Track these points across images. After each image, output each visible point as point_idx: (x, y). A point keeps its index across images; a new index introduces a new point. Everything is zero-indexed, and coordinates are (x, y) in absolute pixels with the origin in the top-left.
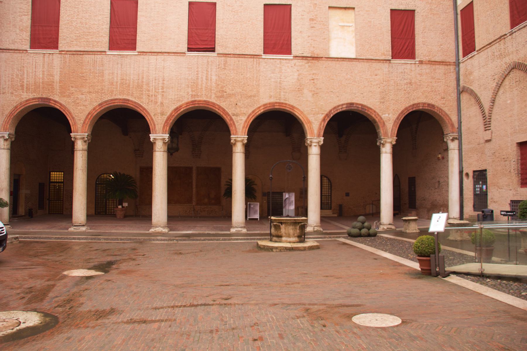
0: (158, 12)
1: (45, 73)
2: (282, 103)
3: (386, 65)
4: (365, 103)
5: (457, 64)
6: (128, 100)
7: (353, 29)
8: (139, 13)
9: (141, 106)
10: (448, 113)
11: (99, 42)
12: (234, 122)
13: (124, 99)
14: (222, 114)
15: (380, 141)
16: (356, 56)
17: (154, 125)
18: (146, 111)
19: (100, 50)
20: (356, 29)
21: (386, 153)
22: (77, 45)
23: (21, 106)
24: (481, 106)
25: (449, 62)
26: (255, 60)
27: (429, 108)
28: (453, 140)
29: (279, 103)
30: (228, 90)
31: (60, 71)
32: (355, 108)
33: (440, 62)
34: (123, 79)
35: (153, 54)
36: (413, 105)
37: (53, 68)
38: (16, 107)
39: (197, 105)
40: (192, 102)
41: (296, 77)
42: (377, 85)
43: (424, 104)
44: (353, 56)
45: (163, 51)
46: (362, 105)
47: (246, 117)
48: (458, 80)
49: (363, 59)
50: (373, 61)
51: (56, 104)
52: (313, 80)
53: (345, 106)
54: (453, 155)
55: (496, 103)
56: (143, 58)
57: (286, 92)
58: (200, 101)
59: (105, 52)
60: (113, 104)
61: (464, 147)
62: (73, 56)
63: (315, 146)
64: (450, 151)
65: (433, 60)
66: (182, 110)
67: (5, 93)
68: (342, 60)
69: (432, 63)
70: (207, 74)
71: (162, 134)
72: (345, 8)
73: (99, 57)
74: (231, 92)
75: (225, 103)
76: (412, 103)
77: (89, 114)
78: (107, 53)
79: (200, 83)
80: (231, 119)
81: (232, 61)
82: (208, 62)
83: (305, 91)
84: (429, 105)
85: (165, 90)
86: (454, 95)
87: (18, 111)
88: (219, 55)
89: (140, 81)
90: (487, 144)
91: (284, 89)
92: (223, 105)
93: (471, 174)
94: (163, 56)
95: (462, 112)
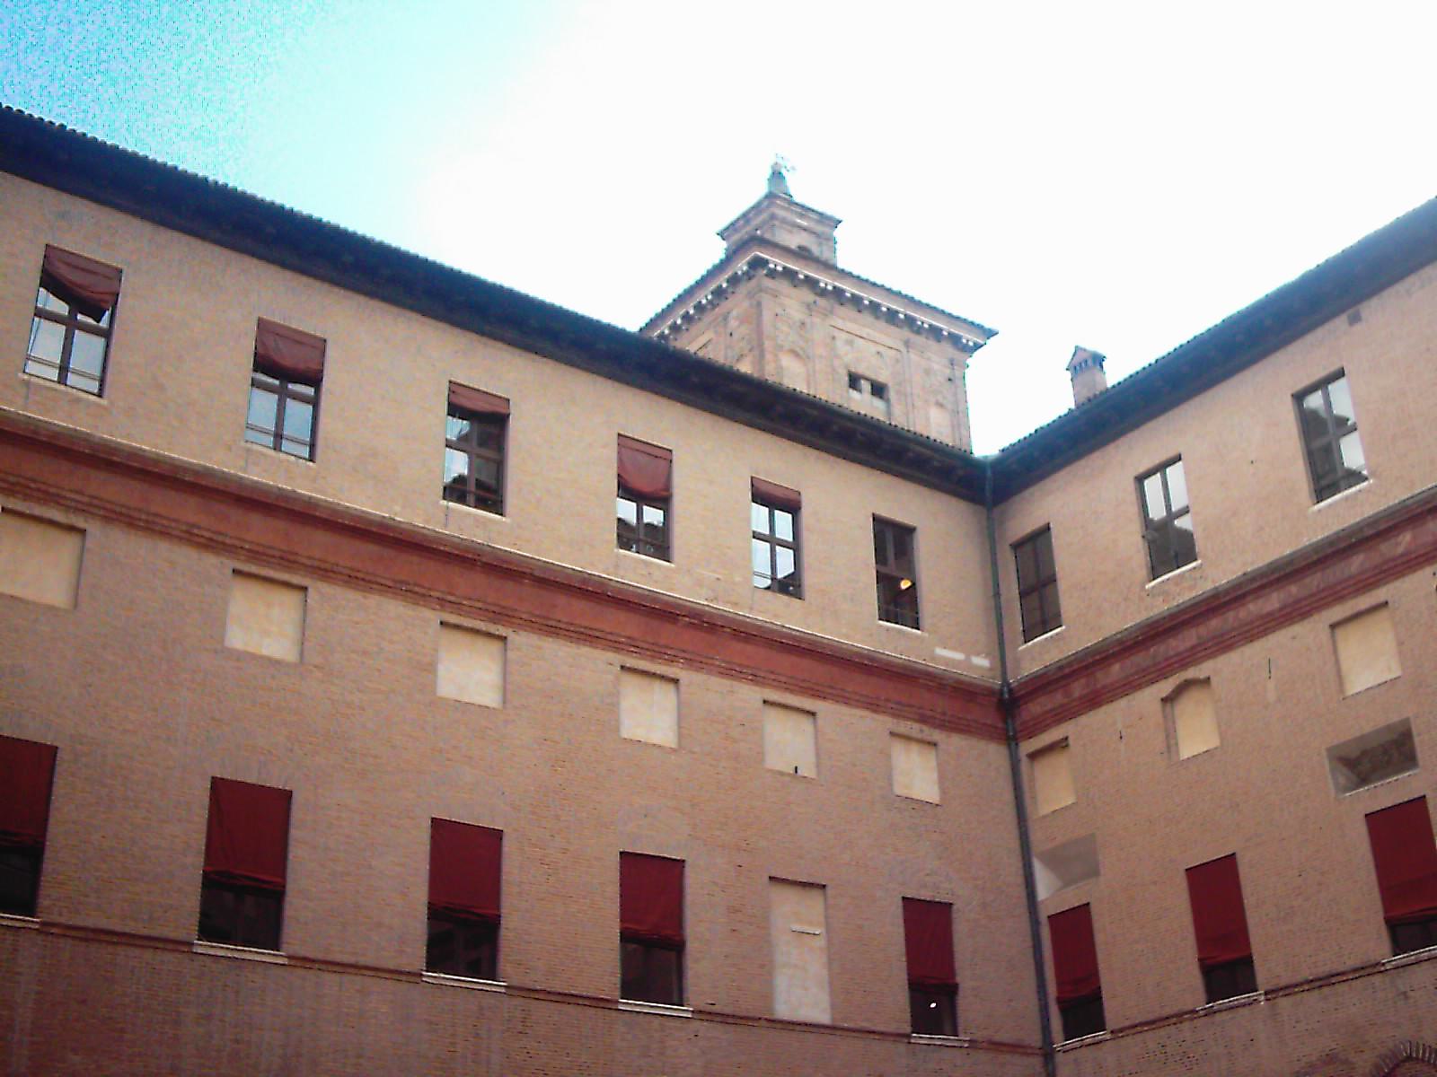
0: (348, 837)
3: (902, 1048)
5: (1048, 1054)
7: (821, 942)
16: (833, 1019)
20: (830, 941)
25: (1032, 1048)
31: (38, 993)
35: (330, 968)
44: (824, 1018)
45: (362, 961)
50: (872, 1036)
65: (998, 1038)
68: (805, 1028)
69: (997, 1046)
73: (169, 959)
81: (542, 1010)
82: (481, 1008)
88: (510, 992)
94: (360, 978)
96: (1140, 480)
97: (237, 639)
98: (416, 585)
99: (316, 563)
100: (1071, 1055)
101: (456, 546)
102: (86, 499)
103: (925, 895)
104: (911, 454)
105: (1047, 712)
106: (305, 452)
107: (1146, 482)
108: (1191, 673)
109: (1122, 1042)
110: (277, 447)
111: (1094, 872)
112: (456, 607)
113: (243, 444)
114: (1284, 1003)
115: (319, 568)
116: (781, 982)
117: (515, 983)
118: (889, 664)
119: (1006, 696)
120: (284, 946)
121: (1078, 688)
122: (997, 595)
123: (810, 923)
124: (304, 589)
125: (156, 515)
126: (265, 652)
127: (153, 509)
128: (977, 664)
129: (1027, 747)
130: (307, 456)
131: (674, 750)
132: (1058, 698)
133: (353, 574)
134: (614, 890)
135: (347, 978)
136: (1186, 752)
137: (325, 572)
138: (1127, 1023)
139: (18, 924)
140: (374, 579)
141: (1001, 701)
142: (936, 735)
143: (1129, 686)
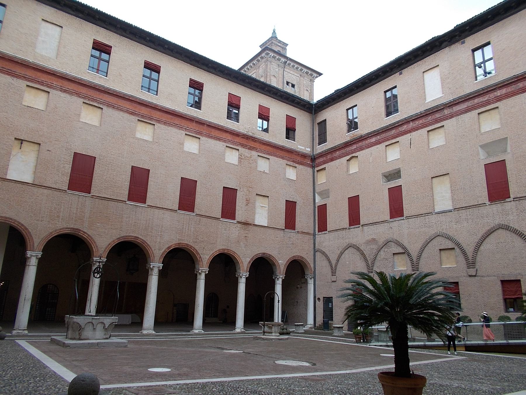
1: (79, 210)
2: (229, 250)
3: (282, 232)
4: (271, 254)
5: (314, 235)
6: (138, 238)
7: (267, 209)
8: (150, 179)
9: (146, 243)
10: (309, 262)
11: (122, 193)
12: (202, 260)
13: (135, 237)
15: (276, 276)
17: (154, 257)
18: (149, 246)
19: (121, 200)
21: (279, 284)
22: (105, 193)
23: (56, 232)
24: (330, 262)
26: (216, 221)
28: (311, 279)
29: (227, 249)
30: (200, 239)
34: (135, 223)
35: (157, 208)
36: (294, 256)
37: (84, 207)
38: (51, 233)
39: (181, 246)
45: (164, 207)
46: (269, 255)
47: (209, 257)
49: (271, 227)
51: (85, 234)
52: (246, 237)
54: (311, 287)
55: (339, 262)
56: (150, 210)
57: (231, 243)
58: (183, 243)
59: (126, 202)
60: (127, 239)
61: (317, 283)
62: (101, 200)
63: (244, 278)
64: (308, 285)
66: (172, 248)
67: (43, 220)
69: (303, 233)
70: (189, 226)
71: (159, 263)
72: (264, 196)
73: (120, 204)
74: (201, 240)
76: (293, 256)
77: (109, 244)
78: (127, 203)
79: (184, 232)
80: (200, 257)
81: (204, 220)
82: (190, 218)
83: (242, 243)
84: (301, 257)
86: (312, 252)
87: (52, 237)
88: (197, 215)
89: (147, 225)
90: (333, 283)
91: (231, 241)
92: (197, 247)
93: (322, 299)
96: (347, 110)
97: (138, 135)
100: (319, 236)
101: (189, 117)
103: (291, 200)
104: (296, 101)
105: (321, 162)
107: (349, 111)
108: (354, 155)
109: (330, 234)
111: (329, 197)
112: (189, 131)
114: (365, 228)
116: (257, 216)
117: (198, 213)
118: (287, 149)
119: (313, 157)
120: (146, 203)
121: (329, 157)
122: (313, 135)
123: (265, 205)
128: (308, 150)
129: (317, 169)
131: (237, 165)
132: (325, 158)
133: (165, 122)
134: (221, 195)
135: (160, 210)
138: (332, 230)
140: (170, 123)
141: (312, 158)
142: (297, 165)
143: (340, 157)
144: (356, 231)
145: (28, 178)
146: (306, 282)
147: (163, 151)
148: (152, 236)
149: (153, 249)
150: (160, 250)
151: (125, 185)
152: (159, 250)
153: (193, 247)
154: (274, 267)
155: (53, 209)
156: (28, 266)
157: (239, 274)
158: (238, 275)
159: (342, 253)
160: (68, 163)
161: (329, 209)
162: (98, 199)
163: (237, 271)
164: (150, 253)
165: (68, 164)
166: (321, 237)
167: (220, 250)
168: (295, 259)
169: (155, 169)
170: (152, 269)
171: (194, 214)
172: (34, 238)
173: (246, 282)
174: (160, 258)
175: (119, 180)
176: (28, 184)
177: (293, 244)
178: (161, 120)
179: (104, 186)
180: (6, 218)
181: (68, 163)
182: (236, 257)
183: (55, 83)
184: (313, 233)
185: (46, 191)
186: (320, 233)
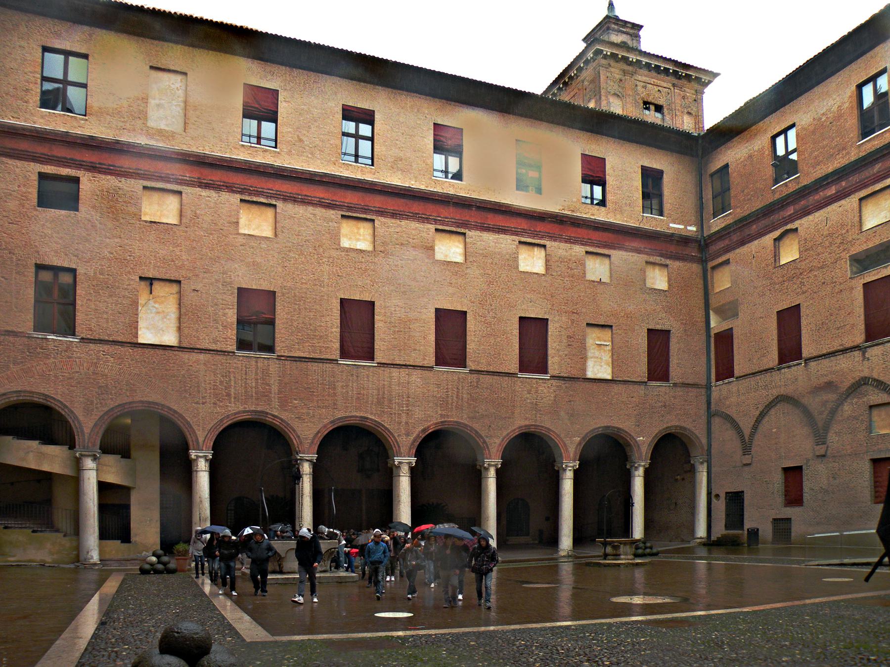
4: (621, 427)
6: (367, 418)
9: (383, 425)
10: (699, 436)
14: (474, 436)
17: (399, 447)
18: (389, 431)
27: (681, 431)
30: (480, 411)
32: (612, 431)
33: (692, 385)
36: (667, 428)
40: (442, 422)
41: (552, 398)
42: (633, 407)
43: (676, 426)
48: (709, 403)
52: (570, 401)
53: (600, 429)
60: (348, 422)
66: (430, 431)
74: (485, 413)
75: (477, 425)
76: (665, 426)
79: (450, 401)
80: (485, 442)
83: (562, 414)
84: (681, 428)
85: (410, 408)
86: (704, 419)
91: (540, 411)
95: (713, 435)
98: (422, 214)
99: (377, 209)
100: (718, 388)
102: (275, 192)
106: (369, 162)
108: (789, 227)
110: (356, 161)
111: (736, 315)
113: (341, 161)
115: (379, 211)
120: (375, 359)
124: (373, 221)
125: (305, 196)
126: (358, 247)
127: (304, 193)
130: (371, 164)
136: (783, 262)
137: (382, 213)
139: (268, 357)
144: (795, 372)
145: (170, 338)
146: (692, 470)
147: (396, 266)
148: (391, 414)
149: (396, 435)
150: (408, 435)
151: (332, 332)
152: (407, 435)
153: (470, 427)
154: (627, 449)
155: (218, 384)
156: (195, 473)
157: (559, 465)
158: (559, 467)
159: (762, 415)
160: (231, 307)
161: (738, 338)
162: (289, 362)
163: (557, 460)
164: (391, 441)
165: (231, 309)
166: (720, 390)
167: (521, 427)
168: (669, 432)
169: (385, 299)
170: (398, 467)
171: (466, 370)
172: (196, 431)
173: (574, 477)
174: (410, 449)
175: (321, 326)
176: (172, 349)
177: (665, 406)
178: (386, 210)
179: (297, 339)
180: (149, 403)
181: (231, 307)
182: (553, 437)
183: (188, 175)
184: (706, 383)
185: (202, 357)
186: (721, 382)
